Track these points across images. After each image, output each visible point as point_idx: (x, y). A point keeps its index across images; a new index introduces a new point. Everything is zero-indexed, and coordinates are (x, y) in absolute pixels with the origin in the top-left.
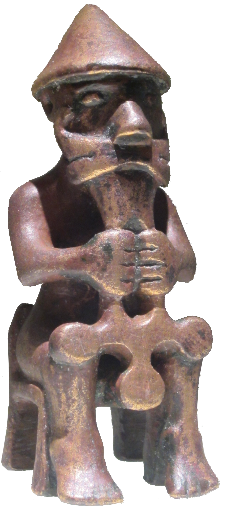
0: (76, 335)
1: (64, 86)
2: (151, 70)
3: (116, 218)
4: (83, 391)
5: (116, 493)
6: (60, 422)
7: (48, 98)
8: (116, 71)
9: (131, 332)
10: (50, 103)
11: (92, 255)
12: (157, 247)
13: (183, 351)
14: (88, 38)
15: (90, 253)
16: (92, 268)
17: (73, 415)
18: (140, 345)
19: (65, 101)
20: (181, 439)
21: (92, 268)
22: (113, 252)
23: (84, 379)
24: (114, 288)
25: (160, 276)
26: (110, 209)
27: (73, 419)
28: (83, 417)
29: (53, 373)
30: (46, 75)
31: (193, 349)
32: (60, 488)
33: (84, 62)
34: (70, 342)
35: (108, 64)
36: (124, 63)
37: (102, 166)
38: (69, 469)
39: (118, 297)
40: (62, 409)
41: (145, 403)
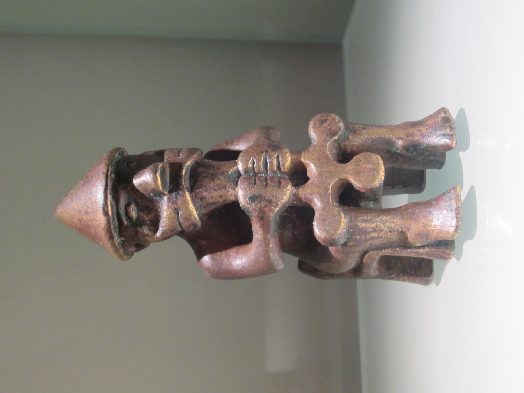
1: (121, 234)
2: (108, 163)
3: (228, 192)
4: (369, 219)
5: (452, 192)
6: (394, 237)
7: (131, 247)
8: (109, 192)
9: (321, 180)
10: (135, 246)
11: (259, 212)
12: (252, 158)
13: (336, 138)
14: (82, 215)
15: (257, 213)
16: (269, 211)
17: (388, 227)
18: (331, 172)
19: (133, 233)
21: (269, 211)
22: (256, 194)
24: (285, 194)
25: (276, 156)
26: (221, 196)
27: (391, 227)
28: (390, 219)
29: (354, 243)
30: (112, 248)
31: (334, 129)
32: (448, 237)
33: (102, 218)
34: (329, 229)
35: (103, 198)
36: (102, 185)
37: (186, 203)
38: (432, 231)
39: (293, 190)
40: (384, 236)
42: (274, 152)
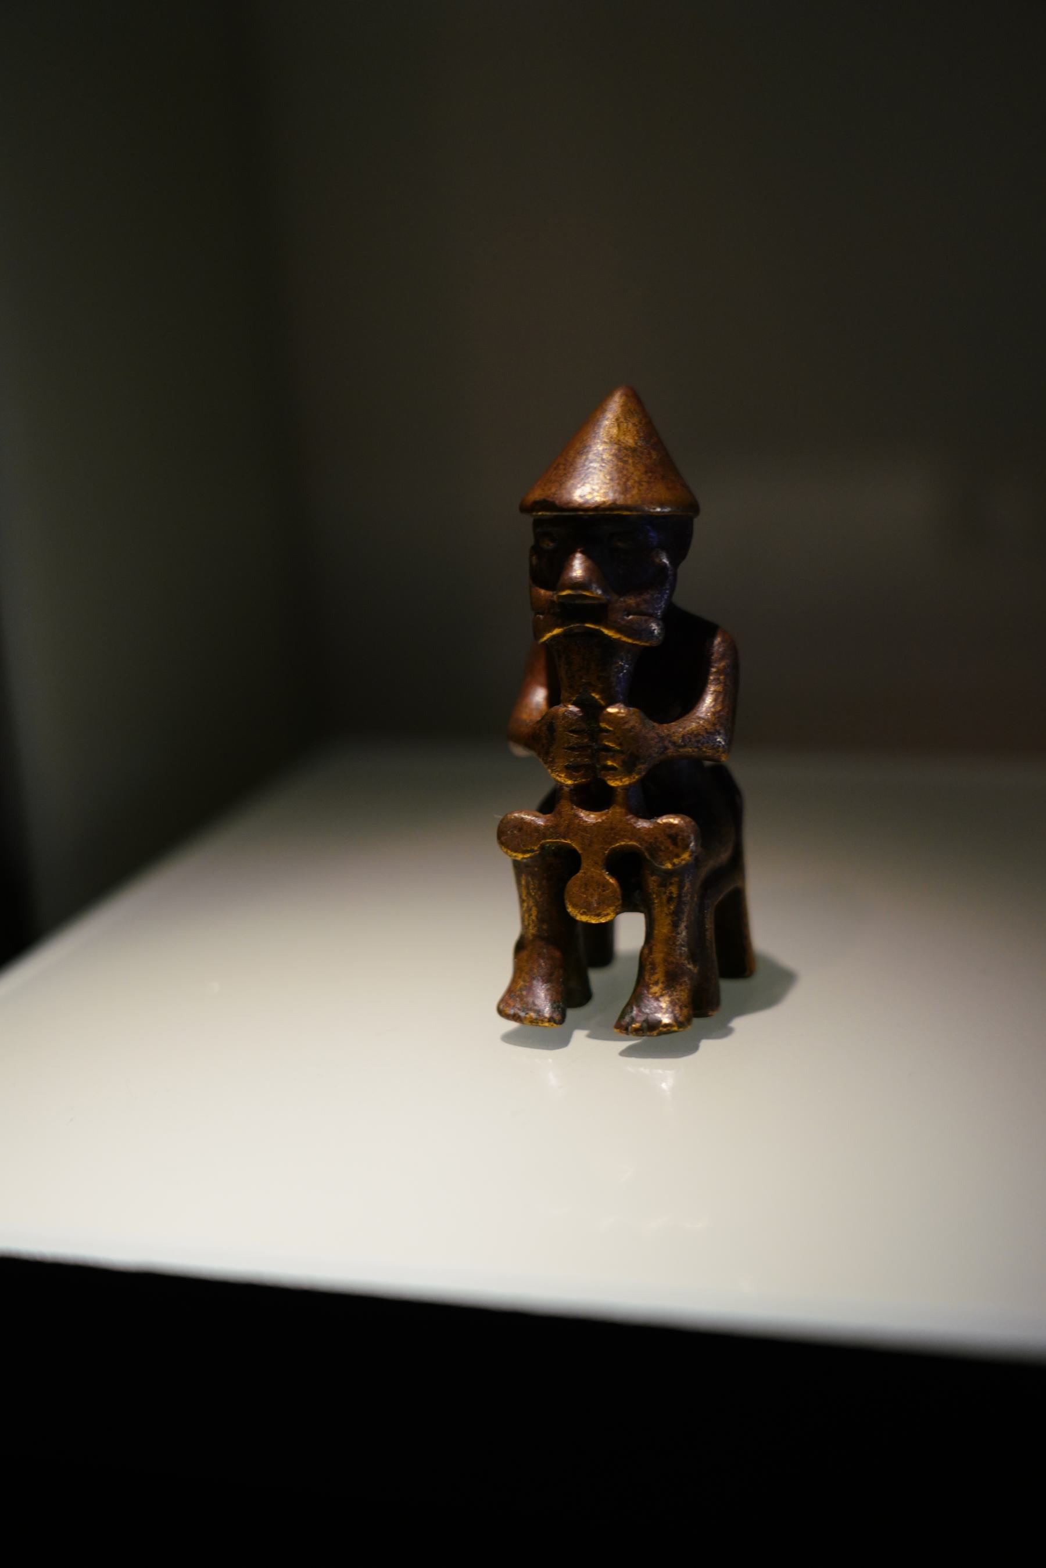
0: (515, 827)
4: (531, 891)
9: (579, 829)
20: (648, 963)
24: (558, 775)
25: (615, 765)
28: (533, 921)
41: (592, 915)
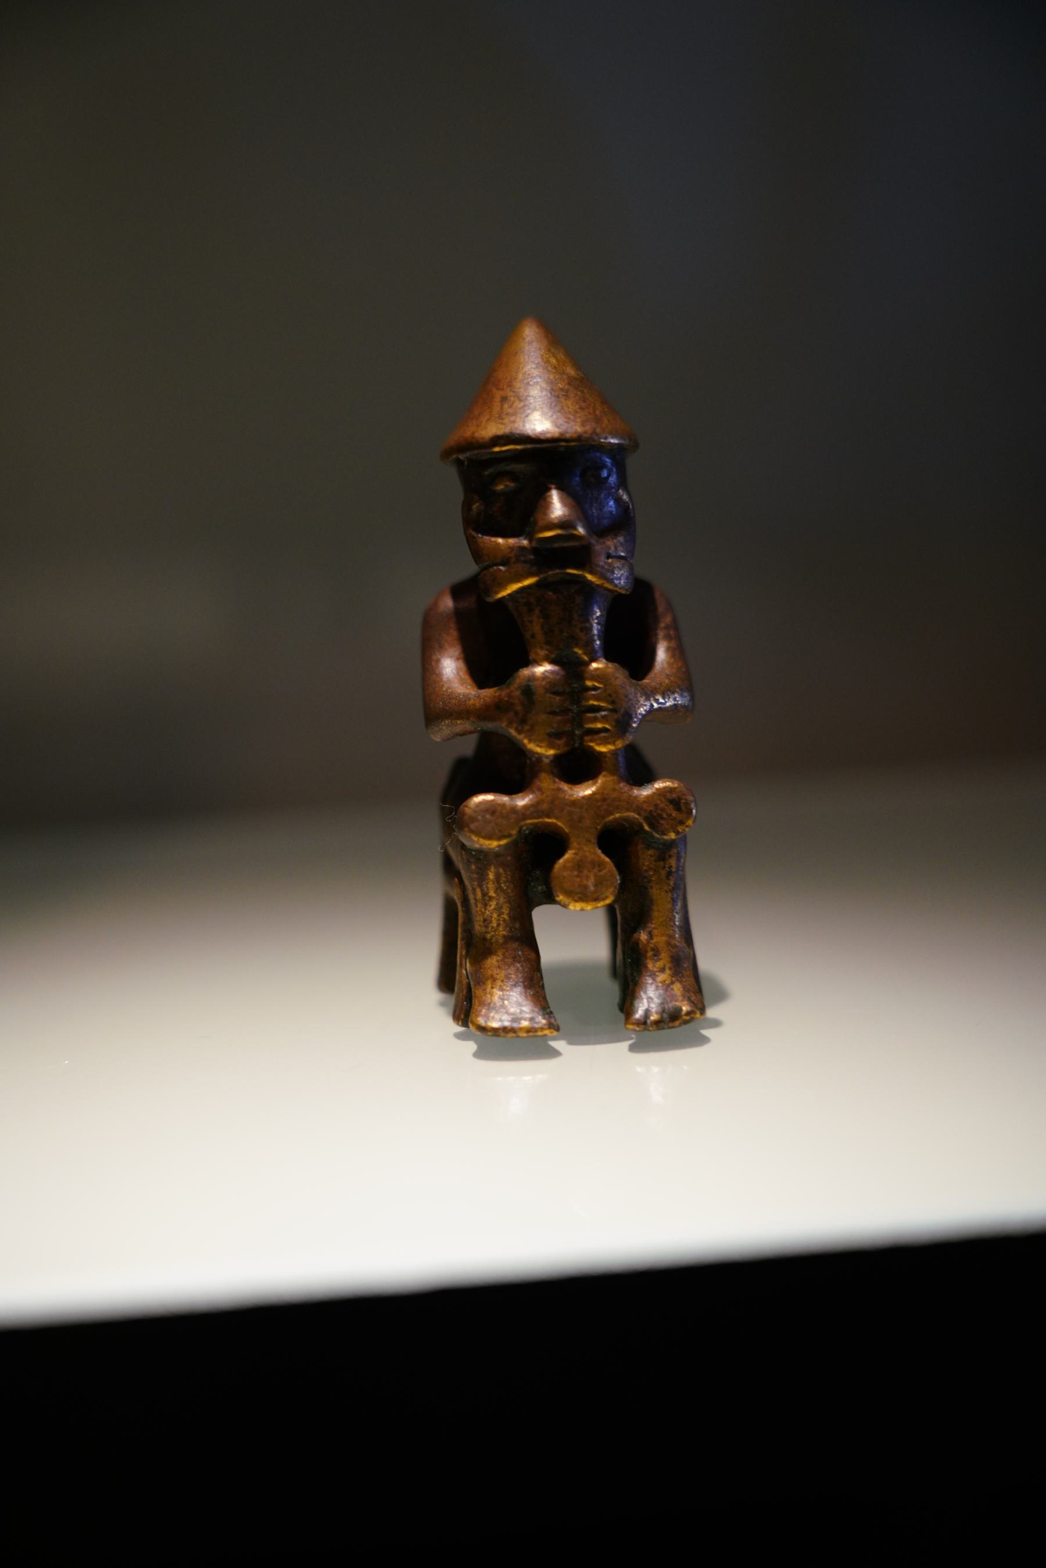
0: (487, 811)
4: (503, 885)
8: (529, 446)
11: (508, 701)
12: (601, 686)
13: (646, 828)
17: (492, 917)
18: (580, 821)
20: (649, 949)
23: (504, 869)
24: (538, 746)
25: (607, 726)
26: (533, 636)
28: (504, 920)
31: (662, 824)
32: (472, 1016)
34: (478, 820)
38: (485, 990)
40: (478, 909)
42: (614, 723)
